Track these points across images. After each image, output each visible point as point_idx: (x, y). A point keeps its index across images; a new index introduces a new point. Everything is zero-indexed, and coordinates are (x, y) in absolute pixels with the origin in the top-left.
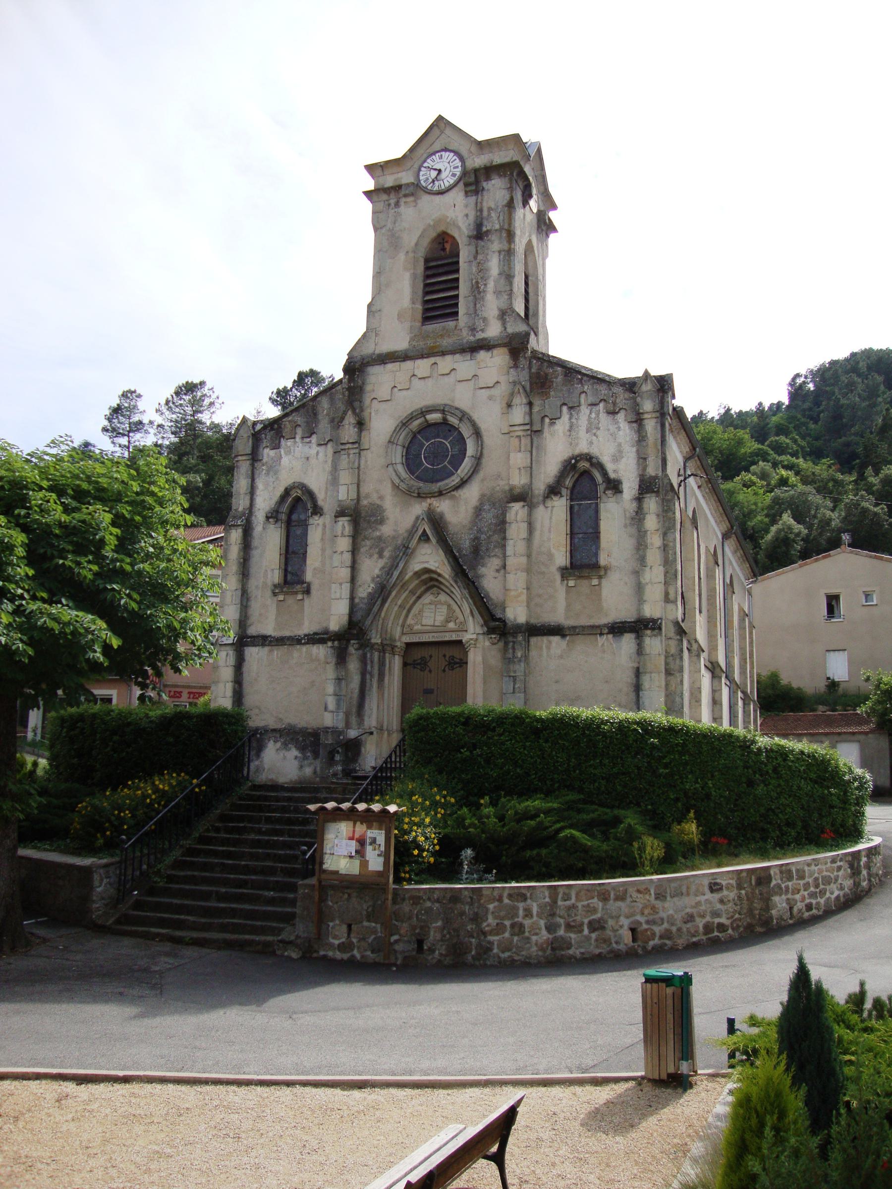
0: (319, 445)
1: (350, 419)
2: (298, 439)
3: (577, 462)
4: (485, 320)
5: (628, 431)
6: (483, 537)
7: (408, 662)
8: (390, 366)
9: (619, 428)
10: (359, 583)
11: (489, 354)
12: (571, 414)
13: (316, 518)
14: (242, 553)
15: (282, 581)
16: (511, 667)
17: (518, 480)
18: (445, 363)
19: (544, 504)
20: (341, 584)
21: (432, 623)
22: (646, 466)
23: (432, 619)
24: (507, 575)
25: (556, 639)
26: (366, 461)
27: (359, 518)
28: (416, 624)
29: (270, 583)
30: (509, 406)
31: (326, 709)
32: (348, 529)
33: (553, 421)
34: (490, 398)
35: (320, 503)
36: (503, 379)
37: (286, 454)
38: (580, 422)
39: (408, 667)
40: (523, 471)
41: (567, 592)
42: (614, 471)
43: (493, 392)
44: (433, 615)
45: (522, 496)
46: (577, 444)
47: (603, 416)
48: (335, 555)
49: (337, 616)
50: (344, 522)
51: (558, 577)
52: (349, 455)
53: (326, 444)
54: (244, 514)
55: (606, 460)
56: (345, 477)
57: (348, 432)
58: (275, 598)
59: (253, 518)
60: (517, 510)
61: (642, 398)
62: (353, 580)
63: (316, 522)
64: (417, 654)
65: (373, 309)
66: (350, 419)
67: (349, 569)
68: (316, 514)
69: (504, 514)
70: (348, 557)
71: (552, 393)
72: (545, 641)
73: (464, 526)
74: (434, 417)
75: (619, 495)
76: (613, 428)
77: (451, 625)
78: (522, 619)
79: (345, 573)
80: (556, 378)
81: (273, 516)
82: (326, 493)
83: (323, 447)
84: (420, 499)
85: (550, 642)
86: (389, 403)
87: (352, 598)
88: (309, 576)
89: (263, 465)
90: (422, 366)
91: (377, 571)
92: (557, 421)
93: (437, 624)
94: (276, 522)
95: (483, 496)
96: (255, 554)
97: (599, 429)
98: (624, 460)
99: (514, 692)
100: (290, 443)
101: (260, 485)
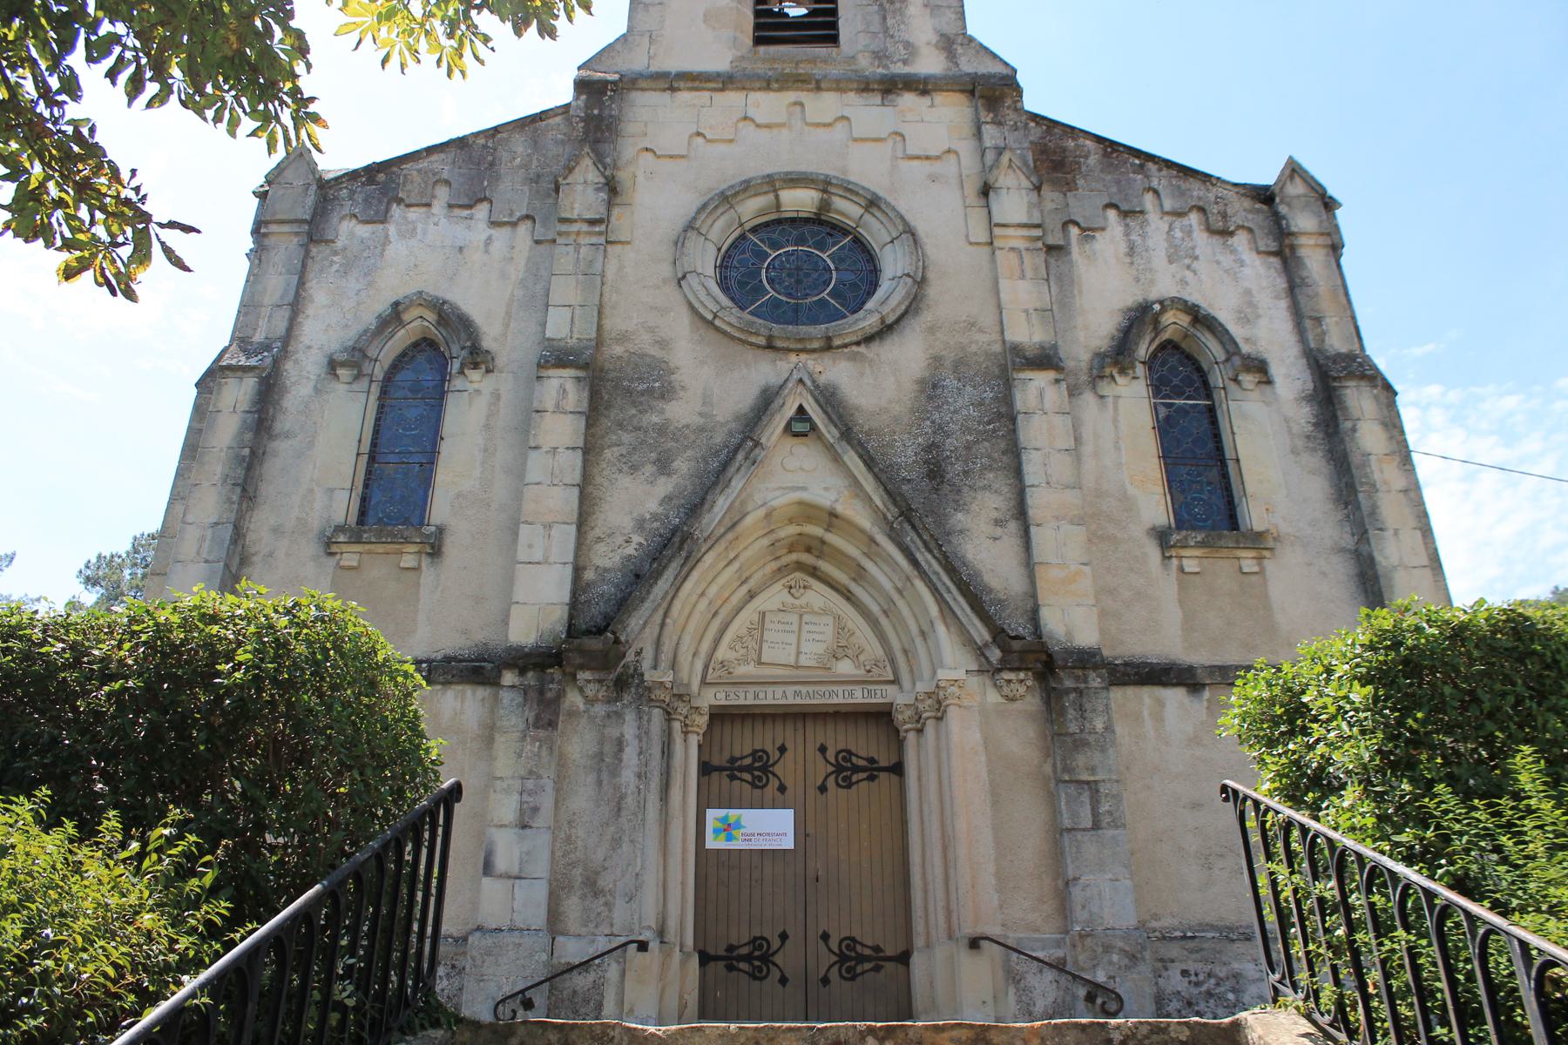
0: (494, 224)
2: (438, 207)
3: (1164, 309)
4: (908, 45)
5: (1262, 270)
6: (951, 443)
7: (716, 762)
8: (684, 96)
9: (1242, 263)
10: (598, 532)
11: (926, 100)
12: (1127, 225)
13: (475, 375)
14: (249, 436)
15: (353, 519)
16: (1081, 760)
17: (1026, 333)
18: (825, 105)
19: (1094, 388)
20: (548, 526)
21: (792, 661)
22: (1324, 333)
24: (1033, 529)
25: (1174, 697)
28: (744, 660)
29: (315, 523)
30: (986, 191)
31: (488, 868)
32: (575, 397)
33: (1088, 232)
34: (933, 178)
35: (487, 343)
36: (966, 148)
37: (402, 235)
38: (1150, 243)
39: (715, 775)
40: (1034, 316)
41: (1182, 587)
42: (1247, 340)
43: (936, 167)
44: (792, 638)
45: (1045, 360)
46: (1152, 282)
47: (1201, 238)
48: (533, 455)
49: (536, 608)
50: (563, 387)
51: (1153, 552)
52: (578, 246)
53: (514, 224)
54: (266, 347)
55: (1224, 315)
56: (565, 290)
57: (582, 197)
58: (332, 562)
59: (289, 366)
60: (1036, 388)
61: (1289, 205)
62: (583, 521)
63: (471, 387)
64: (743, 743)
66: (588, 171)
67: (576, 491)
68: (476, 366)
69: (1007, 399)
70: (571, 464)
71: (1081, 182)
72: (1147, 700)
73: (896, 419)
74: (799, 200)
76: (1227, 260)
77: (845, 668)
78: (1086, 637)
79: (563, 501)
80: (1086, 157)
81: (348, 362)
82: (507, 326)
83: (506, 231)
84: (771, 355)
85: (1161, 703)
86: (684, 162)
87: (578, 570)
88: (440, 509)
89: (336, 253)
90: (767, 105)
91: (652, 506)
92: (1097, 235)
93: (803, 661)
94: (357, 378)
95: (936, 361)
96: (282, 450)
97: (1196, 258)
98: (1263, 322)
99: (1096, 826)
100: (414, 214)
101: (319, 295)
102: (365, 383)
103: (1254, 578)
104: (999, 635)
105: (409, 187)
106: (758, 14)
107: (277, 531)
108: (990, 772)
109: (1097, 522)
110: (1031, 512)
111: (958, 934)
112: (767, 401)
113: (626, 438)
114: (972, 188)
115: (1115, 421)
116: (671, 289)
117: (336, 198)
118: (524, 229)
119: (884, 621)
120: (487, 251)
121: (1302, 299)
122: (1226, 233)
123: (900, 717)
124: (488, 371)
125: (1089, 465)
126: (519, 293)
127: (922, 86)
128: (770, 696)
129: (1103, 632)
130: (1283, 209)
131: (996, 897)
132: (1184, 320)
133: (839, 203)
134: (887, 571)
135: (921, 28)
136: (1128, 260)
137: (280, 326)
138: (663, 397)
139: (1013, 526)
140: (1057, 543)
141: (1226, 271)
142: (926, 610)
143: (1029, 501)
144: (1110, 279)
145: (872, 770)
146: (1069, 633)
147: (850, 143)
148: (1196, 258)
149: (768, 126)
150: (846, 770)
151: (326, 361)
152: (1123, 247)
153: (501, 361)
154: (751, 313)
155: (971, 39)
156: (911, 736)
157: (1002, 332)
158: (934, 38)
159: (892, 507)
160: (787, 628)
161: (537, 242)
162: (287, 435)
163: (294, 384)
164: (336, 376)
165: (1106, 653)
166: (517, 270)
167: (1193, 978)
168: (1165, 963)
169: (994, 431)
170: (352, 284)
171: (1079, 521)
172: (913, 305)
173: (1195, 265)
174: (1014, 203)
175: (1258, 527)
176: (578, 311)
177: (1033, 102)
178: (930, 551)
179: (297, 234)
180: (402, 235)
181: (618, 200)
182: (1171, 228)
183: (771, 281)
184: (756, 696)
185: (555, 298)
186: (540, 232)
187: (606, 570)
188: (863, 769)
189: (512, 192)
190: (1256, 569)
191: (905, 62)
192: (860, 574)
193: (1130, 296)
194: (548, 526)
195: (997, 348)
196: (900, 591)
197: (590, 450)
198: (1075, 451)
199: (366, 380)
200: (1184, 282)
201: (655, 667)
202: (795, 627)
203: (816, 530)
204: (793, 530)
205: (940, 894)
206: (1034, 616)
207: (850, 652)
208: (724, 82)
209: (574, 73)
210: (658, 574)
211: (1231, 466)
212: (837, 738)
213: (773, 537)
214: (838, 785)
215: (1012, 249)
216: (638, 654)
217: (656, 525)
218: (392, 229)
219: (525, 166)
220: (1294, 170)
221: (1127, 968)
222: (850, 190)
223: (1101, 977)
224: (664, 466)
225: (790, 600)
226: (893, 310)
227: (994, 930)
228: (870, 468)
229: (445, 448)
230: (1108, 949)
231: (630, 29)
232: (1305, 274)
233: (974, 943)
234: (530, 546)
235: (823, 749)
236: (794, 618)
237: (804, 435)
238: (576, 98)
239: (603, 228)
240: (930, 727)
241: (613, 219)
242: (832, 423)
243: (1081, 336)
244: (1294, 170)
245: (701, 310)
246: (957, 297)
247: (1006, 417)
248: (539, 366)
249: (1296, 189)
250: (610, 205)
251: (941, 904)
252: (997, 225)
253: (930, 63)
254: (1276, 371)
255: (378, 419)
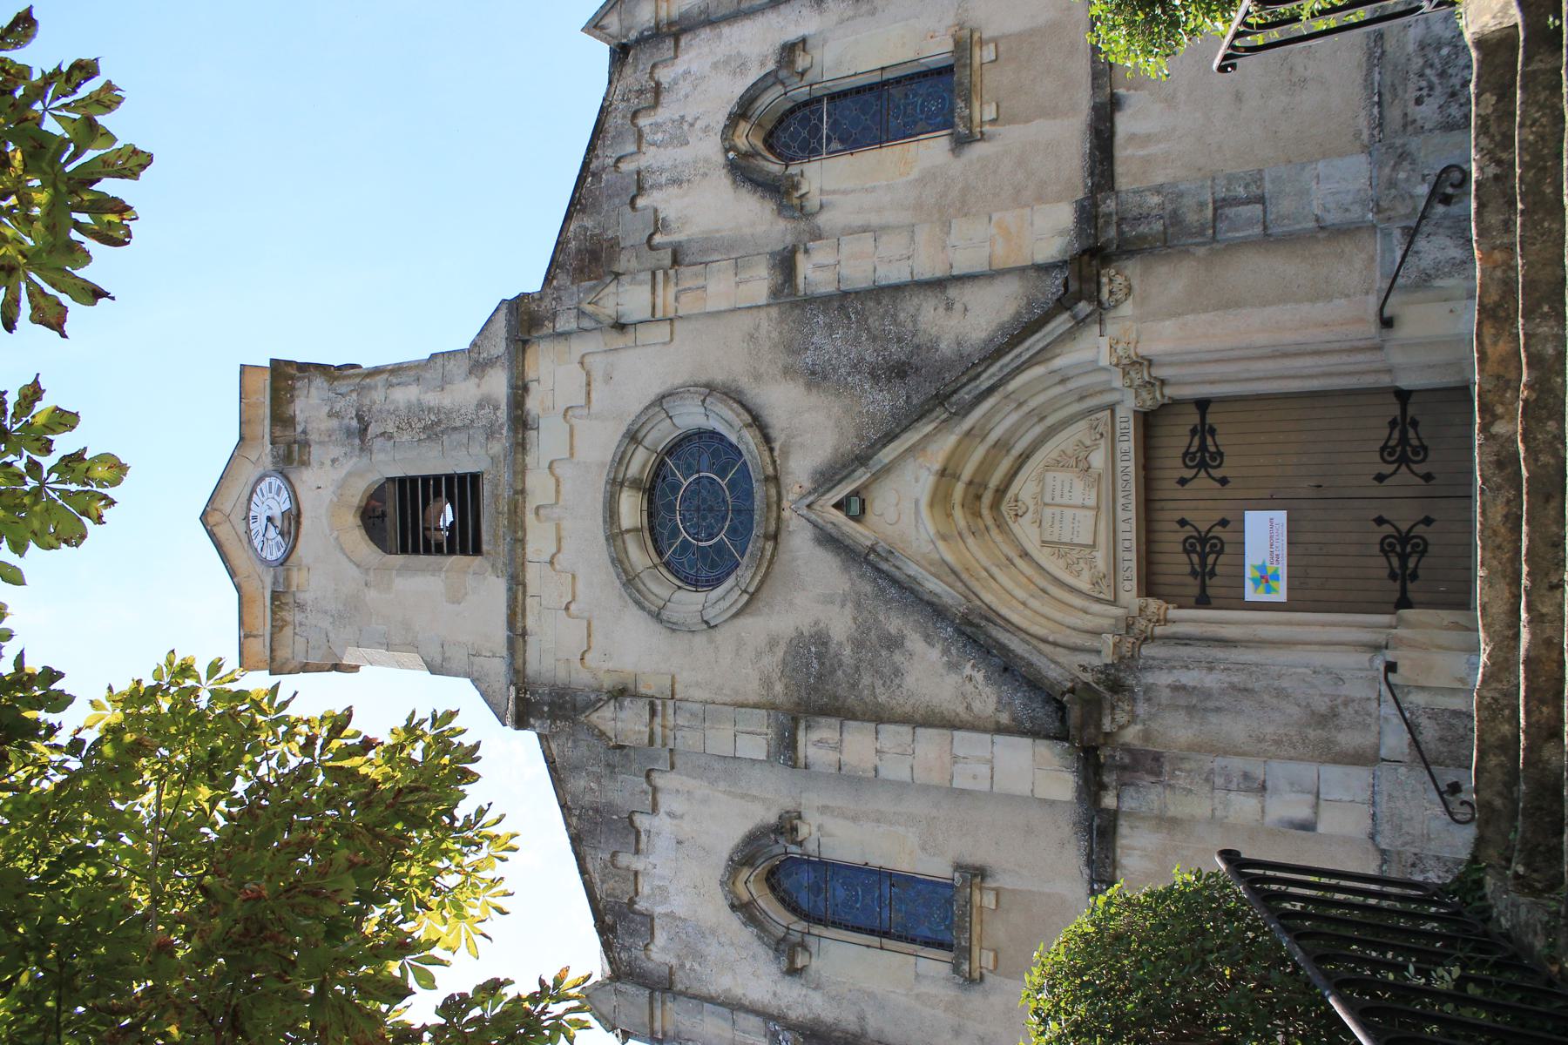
0: (655, 809)
1: (605, 718)
2: (638, 864)
3: (733, 148)
4: (480, 406)
5: (692, 53)
7: (1196, 591)
8: (531, 622)
9: (687, 73)
10: (961, 709)
11: (533, 386)
13: (803, 831)
16: (1192, 218)
17: (759, 284)
18: (538, 485)
20: (955, 759)
23: (1080, 513)
24: (955, 272)
25: (1124, 124)
26: (698, 684)
28: (1091, 562)
29: (948, 993)
30: (620, 326)
31: (1307, 826)
32: (825, 731)
33: (659, 225)
34: (609, 378)
35: (772, 818)
36: (578, 347)
37: (665, 900)
38: (668, 164)
39: (1210, 591)
40: (743, 276)
41: (1012, 120)
42: (762, 64)
44: (1069, 513)
45: (786, 263)
46: (706, 161)
47: (663, 114)
48: (883, 773)
49: (1038, 772)
50: (816, 743)
51: (977, 150)
53: (655, 790)
55: (739, 87)
56: (720, 740)
58: (990, 978)
59: (793, 1015)
60: (814, 273)
61: (629, 29)
62: (951, 724)
64: (1176, 563)
65: (438, 660)
66: (605, 718)
67: (919, 731)
68: (794, 829)
69: (825, 301)
71: (610, 234)
72: (1129, 152)
74: (631, 509)
75: (810, 42)
76: (684, 87)
77: (1098, 459)
78: (1063, 215)
79: (930, 744)
80: (586, 229)
81: (789, 956)
83: (661, 798)
84: (783, 536)
85: (1132, 138)
86: (594, 623)
87: (1000, 730)
88: (937, 867)
89: (682, 966)
90: (538, 542)
91: (934, 654)
93: (1092, 502)
94: (805, 947)
95: (788, 372)
97: (682, 117)
98: (744, 50)
99: (1261, 200)
100: (645, 888)
101: (722, 983)
102: (811, 941)
103: (1001, 48)
104: (1064, 303)
105: (618, 892)
106: (451, 552)
108: (1206, 311)
109: (947, 208)
110: (939, 274)
111: (1377, 340)
112: (829, 540)
113: (866, 680)
114: (618, 340)
115: (845, 193)
116: (719, 635)
117: (629, 964)
118: (659, 780)
119: (1050, 421)
120: (682, 817)
121: (722, 11)
122: (658, 90)
123: (1149, 403)
124: (800, 817)
125: (890, 217)
126: (722, 785)
127: (519, 391)
128: (1128, 535)
129: (1059, 199)
130: (633, 35)
131: (1336, 301)
132: (744, 127)
133: (634, 470)
134: (1000, 418)
135: (464, 393)
136: (685, 185)
137: (754, 1022)
138: (825, 644)
139: (952, 292)
140: (968, 248)
141: (695, 87)
142: (1039, 379)
143: (927, 276)
144: (702, 201)
145: (1204, 431)
146: (1061, 233)
147: (575, 460)
148: (682, 117)
149: (559, 540)
150: (1204, 458)
151: (788, 978)
152: (674, 190)
153: (789, 804)
154: (742, 556)
155: (474, 344)
156: (1168, 391)
157: (759, 307)
158: (474, 380)
159: (935, 414)
160: (1058, 518)
161: (672, 767)
162: (862, 1018)
163: (810, 1010)
164: (804, 968)
165: (1080, 196)
166: (700, 787)
168: (1407, 122)
169: (857, 313)
170: (712, 950)
171: (947, 227)
172: (732, 395)
173: (689, 119)
174: (631, 298)
175: (950, 46)
176: (740, 727)
177: (534, 284)
178: (979, 375)
179: (663, 1003)
180: (665, 900)
181: (632, 687)
182: (654, 144)
183: (710, 537)
184: (1128, 550)
185: (729, 752)
186: (662, 764)
187: (999, 702)
188: (1404, 433)
189: (623, 791)
190: (992, 46)
191: (496, 408)
192: (1002, 446)
193: (721, 182)
194: (955, 759)
195: (774, 312)
196: (1020, 405)
197: (879, 717)
198: (876, 232)
199: (807, 938)
200: (706, 129)
201: (1098, 652)
202: (1057, 510)
203: (959, 490)
204: (958, 513)
205: (1334, 359)
206: (1044, 269)
207: (1082, 455)
208: (517, 583)
209: (509, 730)
210: (1003, 648)
211: (888, 75)
212: (1171, 464)
213: (966, 533)
214: (1219, 466)
215: (676, 299)
216: (1085, 669)
217: (953, 650)
218: (659, 910)
219: (598, 778)
220: (595, 27)
221: (1413, 162)
222: (621, 460)
223: (1423, 190)
224: (894, 643)
225: (1029, 515)
226: (738, 415)
227: (1373, 302)
228: (896, 436)
229: (876, 861)
230: (1392, 184)
231: (467, 675)
232: (696, 10)
233: (1387, 323)
234: (975, 777)
235: (1183, 482)
236: (1048, 511)
237: (863, 502)
238: (533, 728)
239: (658, 702)
240: (1158, 372)
241: (650, 692)
242: (851, 475)
243: (760, 229)
244: (595, 27)
245: (739, 605)
246: (722, 352)
247: (843, 301)
248: (794, 766)
249: (613, 23)
250: (636, 695)
251: (1345, 358)
252: (653, 315)
253: (498, 384)
254: (792, 35)
255: (847, 928)
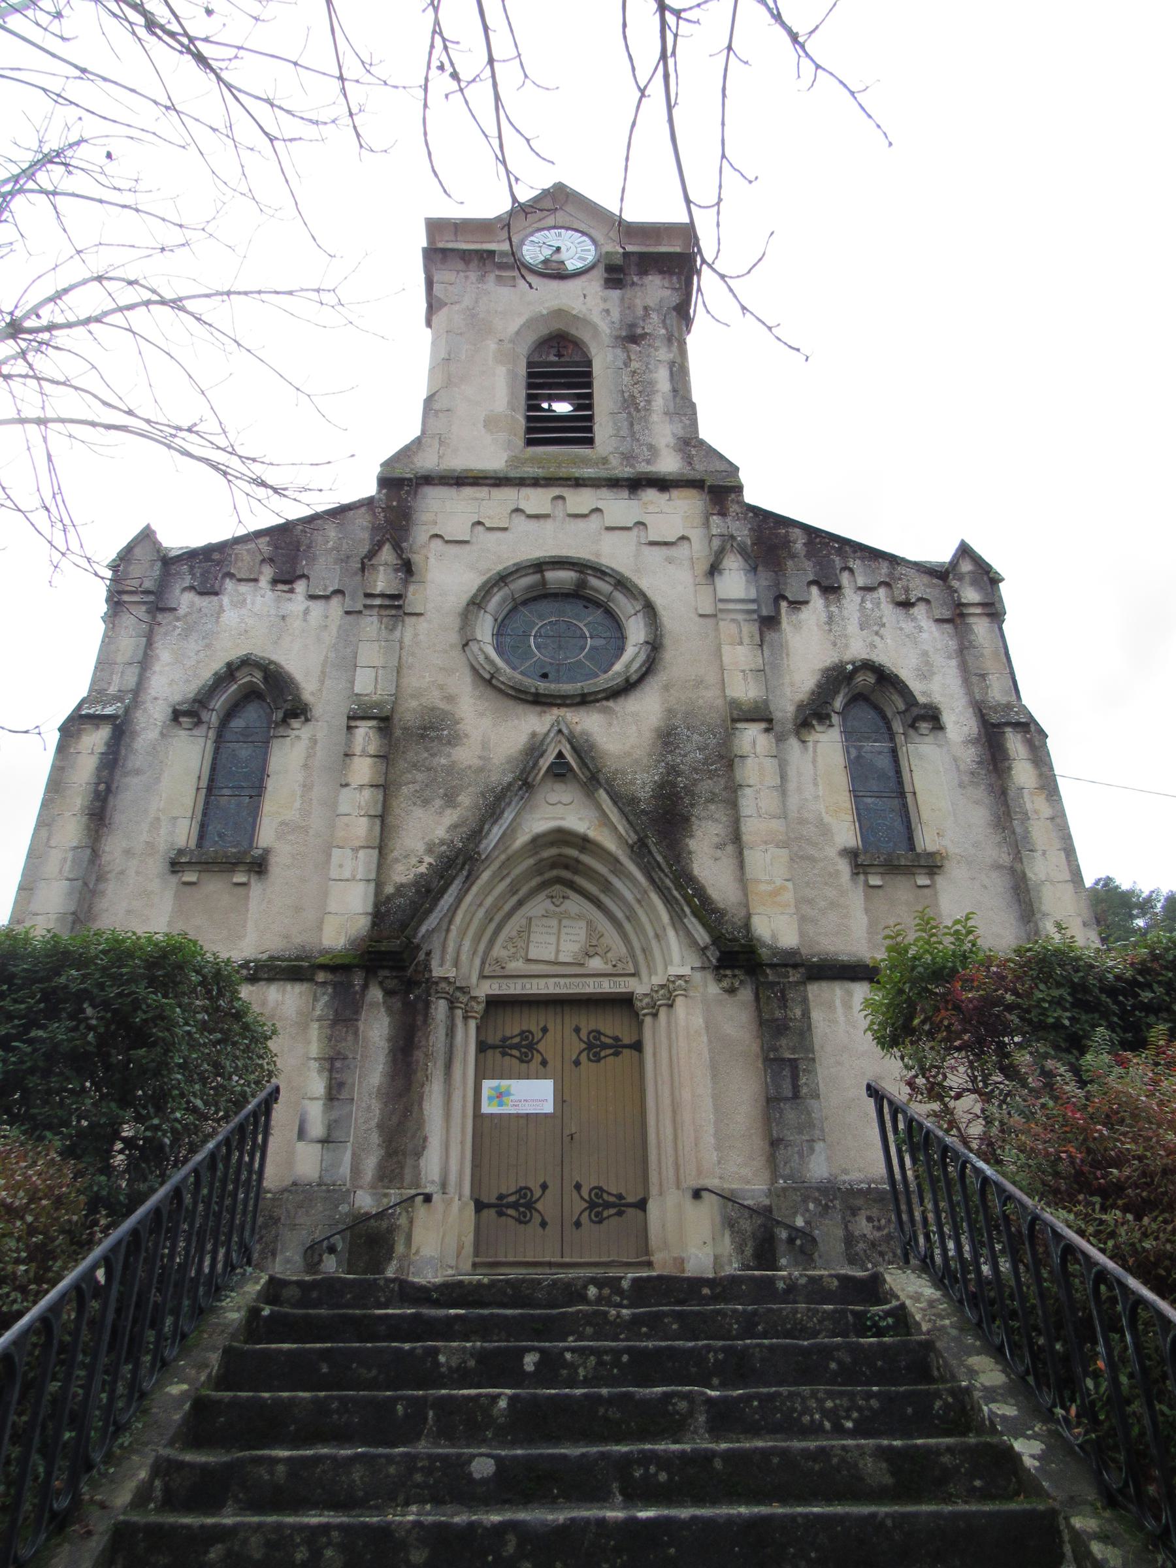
0: (312, 597)
1: (387, 554)
2: (264, 582)
4: (651, 447)
5: (936, 634)
7: (490, 1041)
9: (921, 629)
10: (395, 854)
11: (666, 496)
17: (745, 690)
21: (552, 958)
23: (553, 948)
24: (746, 852)
26: (416, 635)
27: (400, 736)
28: (513, 957)
31: (301, 1134)
33: (797, 605)
34: (670, 560)
36: (696, 535)
38: (845, 613)
39: (490, 1052)
40: (750, 674)
41: (867, 898)
42: (924, 693)
44: (553, 939)
45: (760, 715)
46: (846, 646)
49: (343, 915)
50: (365, 735)
54: (118, 698)
55: (907, 674)
56: (371, 654)
60: (752, 737)
65: (436, 406)
66: (387, 554)
75: (940, 734)
76: (908, 626)
77: (596, 964)
82: (322, 682)
86: (467, 547)
87: (379, 885)
88: (266, 836)
89: (178, 619)
90: (536, 500)
91: (440, 832)
95: (670, 712)
97: (884, 625)
98: (937, 678)
100: (244, 588)
101: (164, 655)
102: (204, 728)
103: (926, 891)
104: (717, 939)
105: (240, 564)
106: (529, 419)
107: (128, 852)
108: (711, 1051)
109: (798, 845)
110: (745, 838)
111: (684, 1185)
112: (534, 750)
113: (420, 777)
114: (704, 566)
115: (814, 762)
116: (456, 654)
117: (178, 573)
118: (335, 601)
119: (628, 927)
120: (305, 620)
121: (970, 660)
122: (906, 605)
123: (639, 1004)
124: (307, 720)
125: (793, 801)
126: (332, 655)
127: (663, 484)
128: (535, 987)
129: (802, 934)
130: (955, 584)
131: (715, 1154)
132: (871, 679)
133: (594, 582)
134: (632, 884)
135: (663, 433)
136: (827, 627)
137: (131, 680)
138: (449, 743)
139: (730, 848)
140: (767, 864)
141: (908, 636)
142: (658, 918)
143: (743, 829)
144: (814, 643)
145: (617, 1047)
146: (773, 936)
147: (604, 532)
148: (884, 625)
149: (537, 517)
150: (596, 1048)
151: (170, 710)
152: (823, 617)
153: (317, 711)
154: (522, 673)
155: (702, 443)
156: (648, 1020)
157: (724, 691)
158: (672, 441)
159: (632, 834)
160: (550, 930)
161: (347, 613)
162: (138, 772)
163: (144, 729)
164: (180, 724)
165: (804, 951)
166: (329, 637)
167: (876, 1223)
168: (854, 1211)
169: (716, 770)
170: (193, 645)
171: (784, 845)
172: (650, 668)
173: (882, 631)
174: (736, 582)
175: (931, 848)
176: (380, 672)
177: (751, 496)
178: (663, 871)
179: (145, 603)
180: (234, 605)
181: (413, 579)
182: (863, 601)
183: (538, 648)
184: (523, 987)
185: (361, 661)
186: (349, 604)
187: (402, 885)
189: (325, 570)
190: (928, 882)
191: (648, 462)
192: (607, 887)
193: (828, 658)
194: (355, 850)
195: (719, 702)
196: (639, 901)
197: (385, 788)
198: (782, 789)
199: (205, 727)
200: (873, 646)
201: (441, 966)
202: (555, 930)
203: (573, 853)
204: (553, 851)
205: (670, 1151)
206: (747, 926)
207: (599, 950)
208: (498, 481)
209: (377, 470)
210: (443, 891)
211: (909, 797)
212: (589, 1022)
213: (538, 857)
214: (589, 1059)
215: (733, 620)
216: (428, 954)
217: (444, 848)
218: (225, 600)
219: (337, 549)
220: (965, 551)
221: (821, 1216)
222: (600, 572)
223: (800, 1222)
224: (450, 800)
225: (552, 908)
226: (636, 671)
227: (713, 1182)
228: (615, 803)
229: (271, 784)
230: (805, 1199)
231: (423, 432)
232: (973, 637)
233: (697, 1194)
234: (341, 866)
235: (577, 1030)
236: (555, 923)
237: (563, 775)
238: (379, 492)
239: (401, 602)
240: (663, 1012)
241: (410, 594)
242: (580, 768)
243: (788, 691)
244: (965, 551)
245: (481, 671)
246: (684, 658)
247: (726, 760)
248: (349, 718)
249: (966, 567)
250: (406, 582)
251: (671, 1160)
252: (721, 601)
253: (669, 464)
254: (948, 719)
255: (214, 759)
